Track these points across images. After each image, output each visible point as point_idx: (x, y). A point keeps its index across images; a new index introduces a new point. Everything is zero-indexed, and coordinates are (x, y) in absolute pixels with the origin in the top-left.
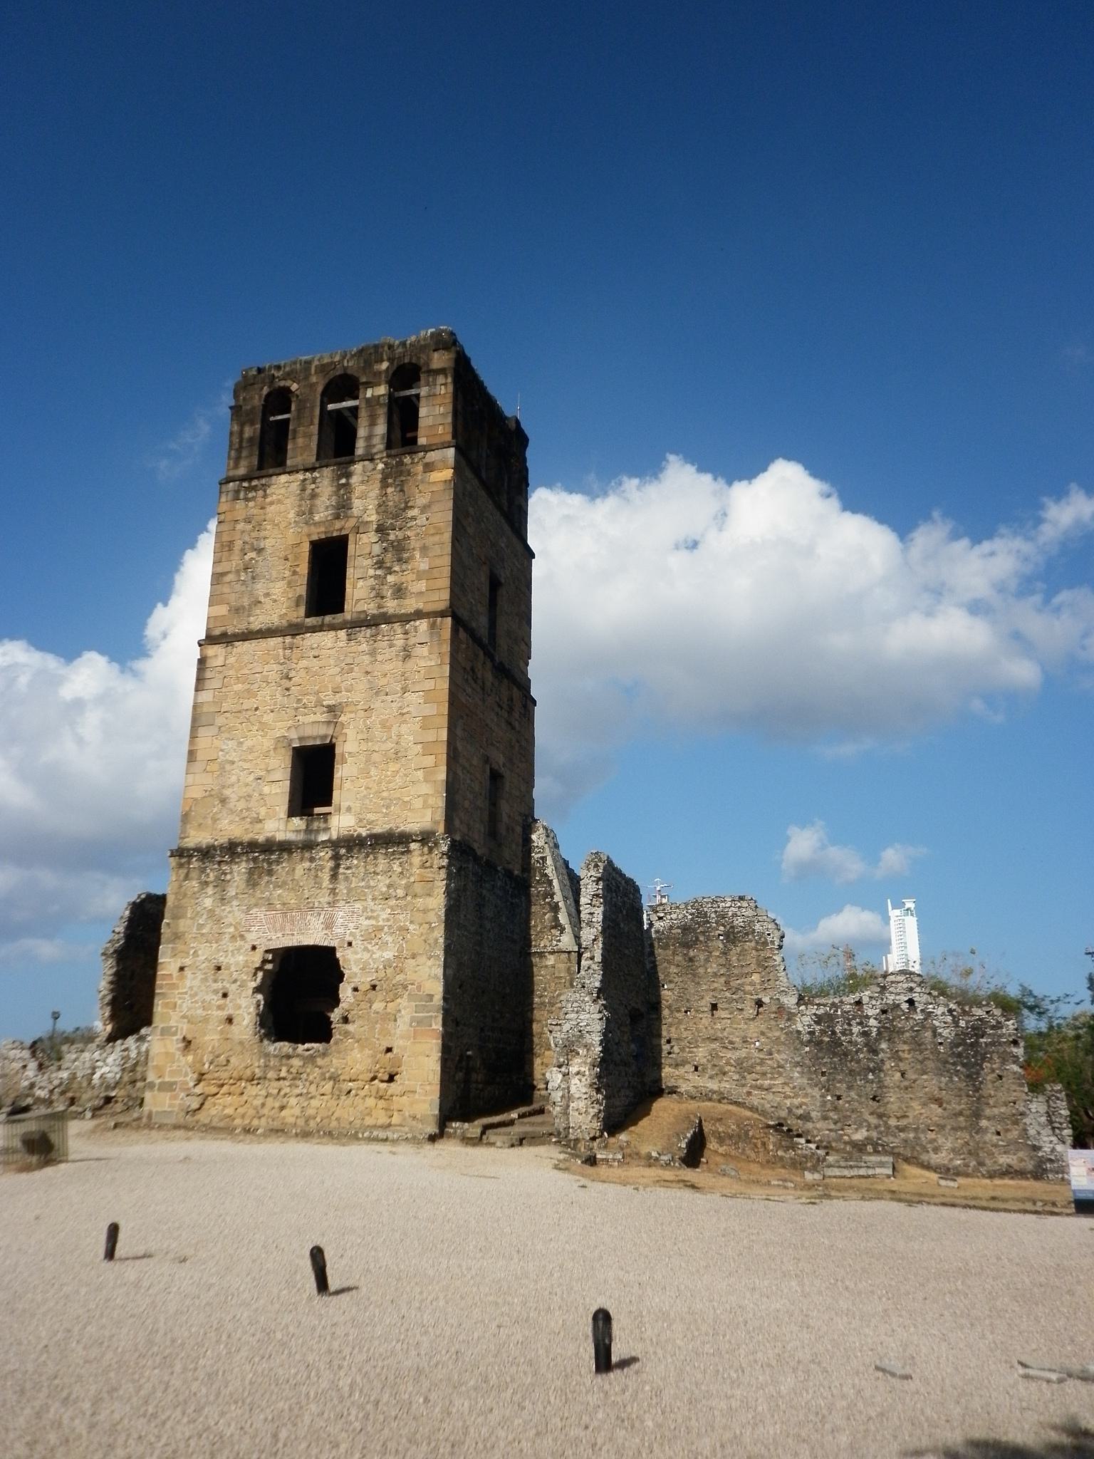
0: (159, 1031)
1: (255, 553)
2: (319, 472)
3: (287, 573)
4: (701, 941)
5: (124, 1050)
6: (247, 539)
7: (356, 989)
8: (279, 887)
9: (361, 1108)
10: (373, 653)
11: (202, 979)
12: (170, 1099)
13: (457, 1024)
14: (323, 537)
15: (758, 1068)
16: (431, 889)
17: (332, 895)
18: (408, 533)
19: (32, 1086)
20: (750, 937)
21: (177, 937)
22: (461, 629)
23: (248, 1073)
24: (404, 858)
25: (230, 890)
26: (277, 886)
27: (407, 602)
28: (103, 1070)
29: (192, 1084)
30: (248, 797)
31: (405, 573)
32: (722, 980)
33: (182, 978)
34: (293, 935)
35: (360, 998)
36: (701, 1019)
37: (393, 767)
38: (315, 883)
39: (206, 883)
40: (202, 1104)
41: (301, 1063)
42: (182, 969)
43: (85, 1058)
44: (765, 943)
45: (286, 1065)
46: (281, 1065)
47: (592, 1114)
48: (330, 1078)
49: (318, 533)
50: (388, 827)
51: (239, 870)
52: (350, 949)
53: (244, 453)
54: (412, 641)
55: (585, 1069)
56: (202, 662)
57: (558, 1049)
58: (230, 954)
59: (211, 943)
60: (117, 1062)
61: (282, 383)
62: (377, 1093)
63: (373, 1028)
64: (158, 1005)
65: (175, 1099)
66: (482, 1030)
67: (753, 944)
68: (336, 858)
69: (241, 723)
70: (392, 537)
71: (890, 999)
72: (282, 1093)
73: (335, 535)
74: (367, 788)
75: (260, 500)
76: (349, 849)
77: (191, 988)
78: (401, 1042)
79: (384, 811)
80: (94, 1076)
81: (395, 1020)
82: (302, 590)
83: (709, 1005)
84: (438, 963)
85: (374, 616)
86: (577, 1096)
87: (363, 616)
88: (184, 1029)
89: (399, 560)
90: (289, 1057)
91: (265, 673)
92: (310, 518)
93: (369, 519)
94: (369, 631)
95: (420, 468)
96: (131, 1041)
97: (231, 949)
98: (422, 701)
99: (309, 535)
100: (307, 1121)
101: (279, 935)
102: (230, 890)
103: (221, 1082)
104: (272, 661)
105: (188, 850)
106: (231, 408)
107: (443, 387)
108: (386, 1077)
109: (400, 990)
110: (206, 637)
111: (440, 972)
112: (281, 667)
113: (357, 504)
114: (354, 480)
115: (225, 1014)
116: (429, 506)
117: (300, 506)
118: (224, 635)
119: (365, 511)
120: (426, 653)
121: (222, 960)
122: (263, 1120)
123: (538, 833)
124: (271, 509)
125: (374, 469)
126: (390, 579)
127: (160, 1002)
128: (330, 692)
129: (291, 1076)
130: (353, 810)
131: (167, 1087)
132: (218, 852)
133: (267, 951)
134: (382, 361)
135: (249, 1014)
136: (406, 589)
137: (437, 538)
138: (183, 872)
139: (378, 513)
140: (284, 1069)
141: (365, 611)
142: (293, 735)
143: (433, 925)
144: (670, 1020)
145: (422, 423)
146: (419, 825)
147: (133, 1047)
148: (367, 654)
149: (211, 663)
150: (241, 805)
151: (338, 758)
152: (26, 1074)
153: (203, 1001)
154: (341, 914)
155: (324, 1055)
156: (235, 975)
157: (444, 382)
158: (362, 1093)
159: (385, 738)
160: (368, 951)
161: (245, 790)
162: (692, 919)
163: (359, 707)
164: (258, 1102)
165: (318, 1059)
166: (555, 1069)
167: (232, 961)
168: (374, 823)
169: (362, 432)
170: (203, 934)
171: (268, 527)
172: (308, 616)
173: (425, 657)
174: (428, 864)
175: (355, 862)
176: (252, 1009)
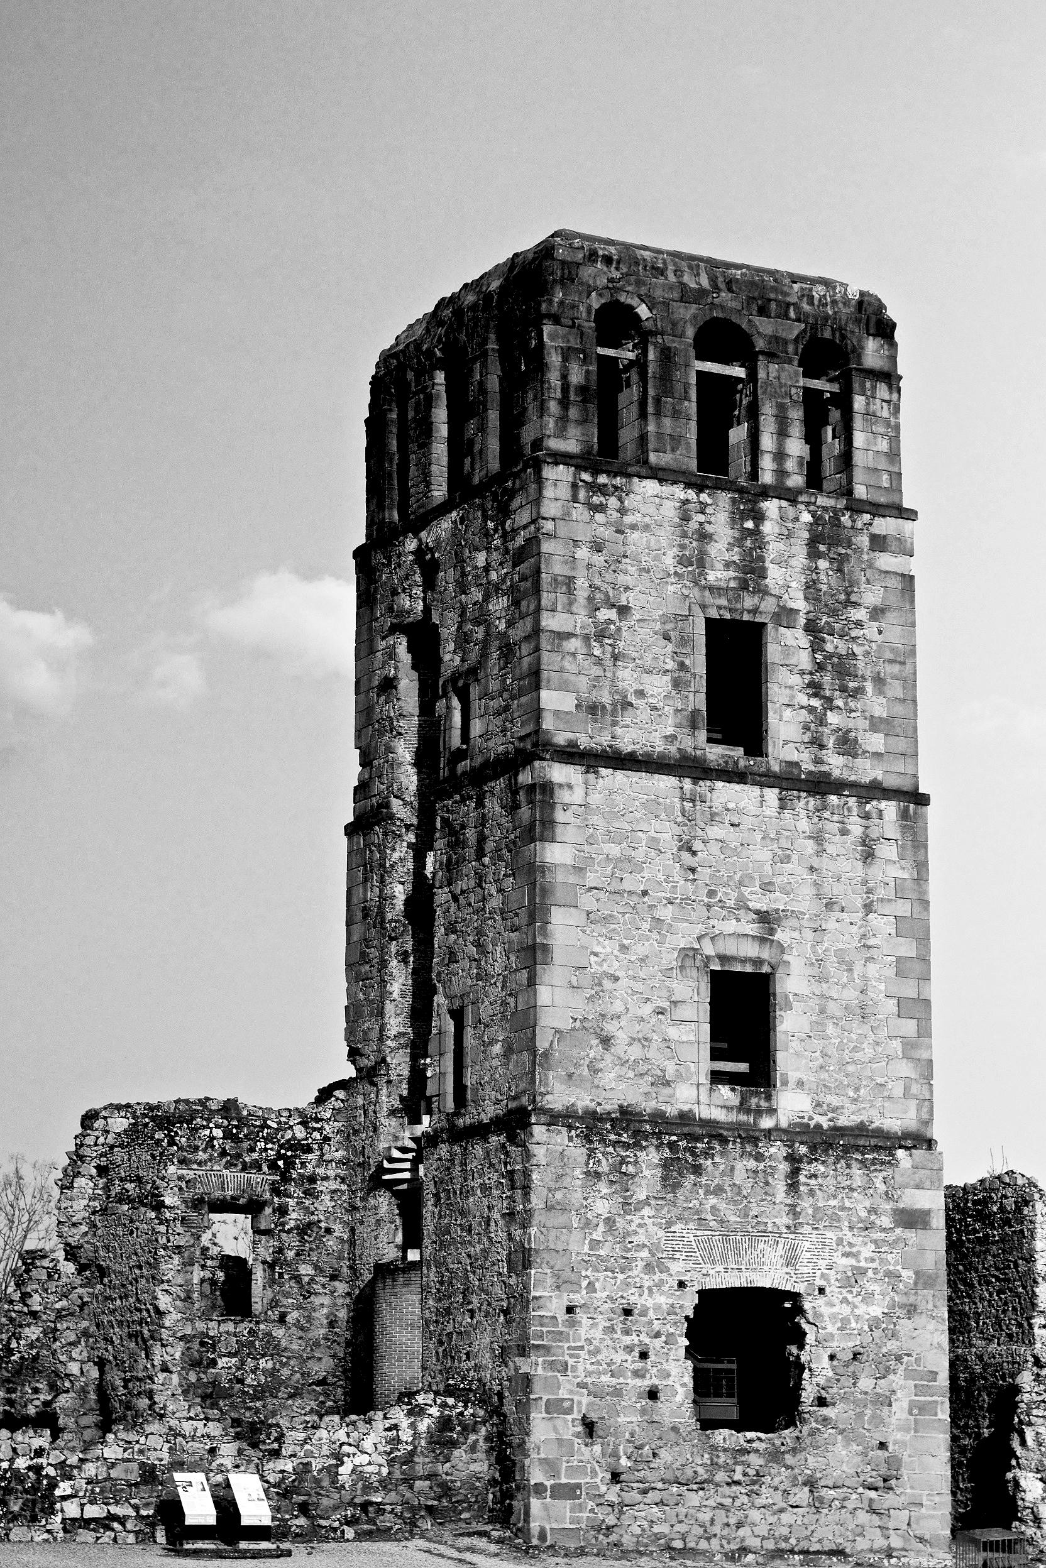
0: (542, 1404)
1: (614, 610)
2: (709, 495)
3: (671, 665)
6: (598, 582)
7: (832, 1357)
8: (712, 1193)
9: (851, 1526)
10: (818, 838)
12: (572, 1510)
14: (727, 616)
17: (791, 1216)
23: (689, 1472)
24: (889, 1172)
25: (637, 1189)
27: (859, 762)
28: (357, 1461)
29: (603, 1489)
31: (853, 715)
33: (573, 1324)
35: (841, 1371)
37: (858, 1028)
39: (598, 1175)
41: (761, 1462)
42: (570, 1310)
43: (320, 1439)
45: (743, 1463)
46: (736, 1463)
49: (719, 608)
51: (650, 1158)
52: (822, 1300)
53: (574, 413)
58: (646, 1292)
59: (613, 1272)
60: (381, 1448)
61: (623, 298)
63: (860, 1416)
68: (792, 1158)
69: (624, 914)
70: (829, 647)
72: (738, 1503)
73: (746, 617)
74: (824, 1055)
76: (813, 1148)
77: (589, 1341)
78: (899, 1436)
79: (851, 1094)
80: (341, 1470)
81: (890, 1405)
82: (699, 701)
84: (940, 1327)
85: (811, 772)
87: (796, 772)
88: (584, 1401)
89: (843, 689)
91: (652, 834)
92: (700, 574)
94: (812, 802)
95: (864, 541)
97: (647, 1284)
98: (893, 932)
99: (703, 607)
101: (720, 1268)
102: (637, 1189)
104: (663, 816)
109: (893, 1363)
111: (944, 1339)
112: (677, 830)
114: (768, 528)
115: (646, 1383)
118: (573, 744)
121: (633, 1298)
122: (715, 1542)
125: (797, 519)
126: (833, 718)
127: (540, 1360)
128: (757, 889)
130: (806, 1087)
131: (568, 1492)
133: (698, 1292)
135: (684, 1385)
136: (856, 741)
137: (895, 669)
139: (806, 599)
141: (796, 764)
142: (709, 949)
145: (859, 458)
146: (899, 1122)
147: (405, 1423)
148: (810, 837)
149: (563, 796)
150: (635, 1052)
154: (807, 1245)
155: (794, 1451)
156: (657, 1326)
157: (887, 397)
159: (845, 980)
161: (638, 1028)
163: (805, 923)
164: (705, 1517)
165: (787, 1456)
166: (1031, 1475)
167: (650, 1303)
168: (839, 1111)
169: (767, 442)
171: (632, 570)
175: (822, 1168)
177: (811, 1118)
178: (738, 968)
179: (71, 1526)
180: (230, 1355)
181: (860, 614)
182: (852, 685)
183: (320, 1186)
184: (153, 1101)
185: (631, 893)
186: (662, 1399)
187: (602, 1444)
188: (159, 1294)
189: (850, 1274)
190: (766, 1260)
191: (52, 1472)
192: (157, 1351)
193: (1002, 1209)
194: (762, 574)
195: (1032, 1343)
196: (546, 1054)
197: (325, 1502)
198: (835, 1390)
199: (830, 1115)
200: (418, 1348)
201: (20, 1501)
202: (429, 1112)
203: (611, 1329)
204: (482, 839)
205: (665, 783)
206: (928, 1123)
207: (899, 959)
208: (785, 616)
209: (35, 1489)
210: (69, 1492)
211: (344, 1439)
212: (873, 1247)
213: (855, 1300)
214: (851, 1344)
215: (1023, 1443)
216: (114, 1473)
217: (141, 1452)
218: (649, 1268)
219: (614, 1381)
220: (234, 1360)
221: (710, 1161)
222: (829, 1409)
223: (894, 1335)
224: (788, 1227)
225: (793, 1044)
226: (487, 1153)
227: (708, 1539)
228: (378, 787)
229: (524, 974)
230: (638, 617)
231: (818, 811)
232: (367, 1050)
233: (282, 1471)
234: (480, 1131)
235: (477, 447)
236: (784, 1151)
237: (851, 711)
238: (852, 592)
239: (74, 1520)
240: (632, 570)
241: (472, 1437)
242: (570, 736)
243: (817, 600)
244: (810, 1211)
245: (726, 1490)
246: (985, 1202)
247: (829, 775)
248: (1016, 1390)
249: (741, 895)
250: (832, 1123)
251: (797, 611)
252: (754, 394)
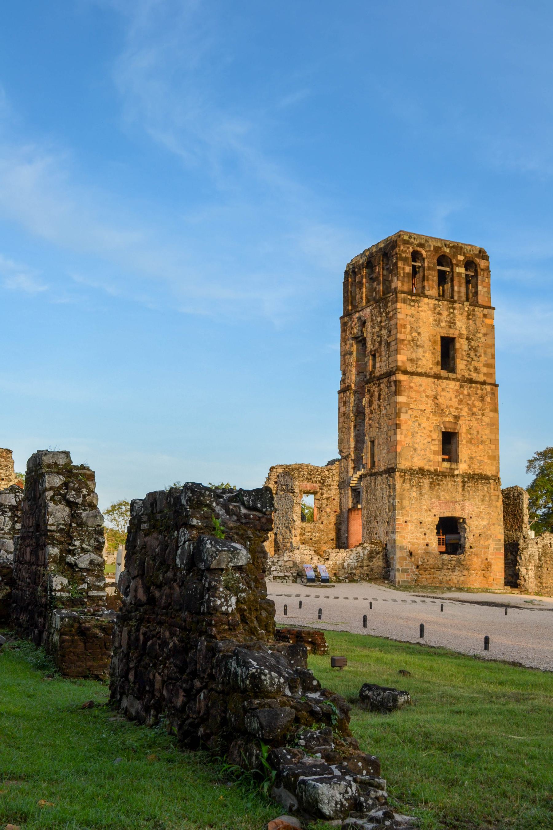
3: (431, 348)
7: (474, 535)
21: (403, 508)
23: (437, 566)
24: (488, 485)
29: (415, 570)
33: (407, 526)
39: (413, 486)
51: (426, 482)
52: (471, 520)
55: (533, 568)
63: (481, 551)
68: (463, 482)
70: (473, 343)
71: (545, 542)
73: (451, 336)
76: (469, 479)
78: (490, 557)
85: (467, 378)
89: (476, 355)
90: (451, 560)
93: (463, 333)
113: (458, 324)
115: (426, 542)
124: (422, 313)
138: (402, 479)
140: (449, 565)
147: (361, 552)
149: (404, 384)
150: (423, 453)
153: (416, 536)
164: (440, 578)
167: (427, 520)
169: (456, 288)
179: (275, 578)
180: (309, 532)
181: (480, 335)
182: (478, 354)
183: (332, 487)
184: (288, 464)
188: (294, 516)
192: (293, 531)
193: (513, 496)
194: (455, 324)
195: (522, 532)
196: (399, 453)
200: (361, 531)
202: (363, 467)
204: (380, 395)
205: (431, 380)
206: (498, 473)
208: (460, 335)
210: (275, 569)
215: (521, 559)
216: (286, 564)
219: (417, 541)
220: (310, 534)
223: (490, 530)
226: (382, 479)
228: (347, 381)
229: (393, 432)
232: (344, 451)
234: (381, 474)
235: (377, 289)
239: (276, 577)
240: (421, 322)
241: (378, 556)
243: (469, 331)
245: (446, 570)
246: (508, 494)
248: (519, 545)
252: (453, 275)
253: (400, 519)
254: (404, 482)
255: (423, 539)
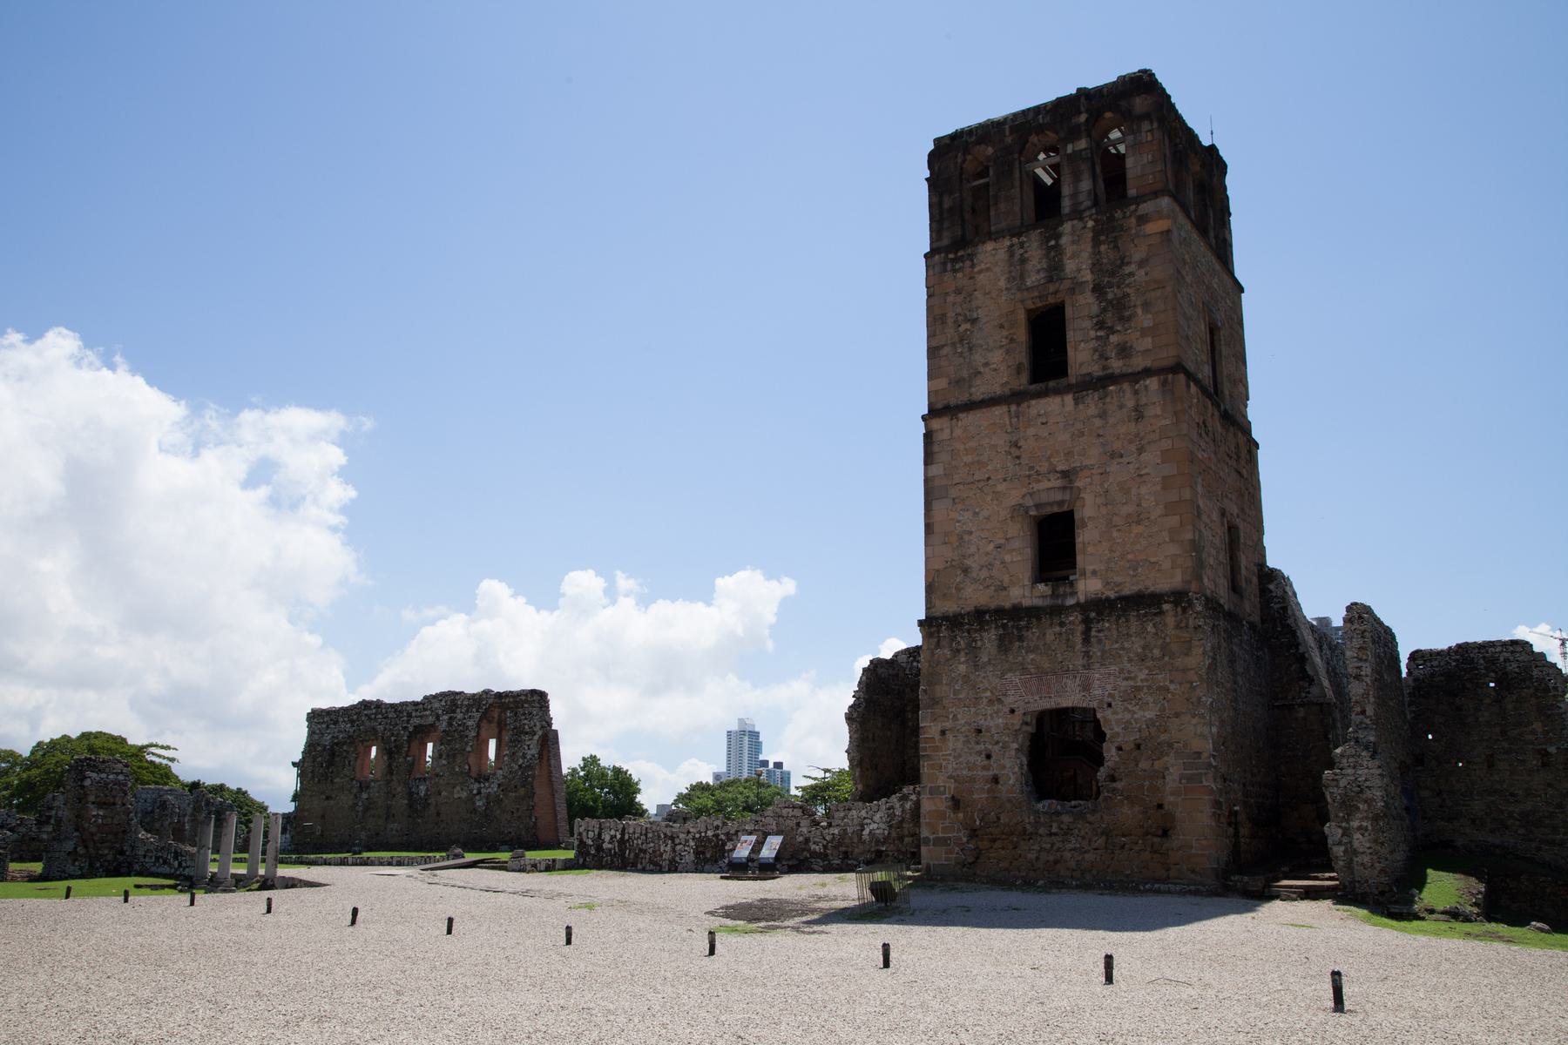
3: (1005, 342)
4: (1468, 689)
5: (889, 809)
6: (959, 310)
7: (1119, 749)
10: (1103, 415)
11: (964, 741)
12: (946, 853)
13: (1225, 780)
15: (1547, 822)
16: (1190, 649)
18: (1128, 290)
19: (807, 840)
20: (1528, 683)
21: (935, 702)
22: (1192, 384)
24: (1158, 619)
26: (1029, 651)
28: (871, 827)
29: (965, 839)
30: (990, 566)
32: (1498, 729)
34: (1050, 697)
36: (1475, 770)
37: (1137, 529)
38: (1067, 647)
39: (958, 651)
40: (977, 858)
42: (943, 733)
44: (1547, 690)
46: (1052, 821)
47: (1378, 869)
48: (1102, 834)
50: (1135, 589)
52: (1109, 711)
53: (946, 225)
54: (1143, 401)
56: (928, 437)
57: (1336, 804)
62: (1152, 846)
64: (923, 766)
65: (951, 853)
66: (1244, 785)
67: (1532, 690)
68: (1087, 622)
70: (1110, 296)
72: (1055, 848)
73: (1051, 300)
74: (1111, 551)
75: (967, 270)
76: (1099, 614)
77: (954, 750)
79: (1131, 573)
80: (864, 833)
81: (1164, 778)
82: (1022, 355)
83: (1484, 756)
84: (1203, 721)
85: (1100, 379)
86: (1361, 850)
87: (1087, 379)
89: (1121, 319)
90: (1058, 813)
93: (1084, 279)
94: (1096, 395)
95: (1133, 220)
96: (894, 799)
97: (989, 712)
98: (1159, 461)
99: (1022, 301)
100: (1083, 874)
103: (994, 837)
105: (936, 618)
106: (926, 179)
107: (1149, 134)
108: (1160, 832)
110: (929, 411)
113: (1070, 266)
114: (1064, 240)
115: (991, 773)
116: (1147, 260)
117: (1010, 272)
119: (1079, 270)
120: (1159, 413)
123: (1275, 582)
125: (1085, 227)
126: (1114, 339)
127: (926, 764)
129: (1063, 833)
132: (966, 621)
133: (1024, 714)
134: (1080, 113)
135: (1013, 773)
136: (1131, 347)
137: (1158, 293)
139: (1092, 272)
140: (1055, 825)
142: (1029, 502)
143: (1194, 684)
144: (1439, 772)
145: (1130, 174)
147: (898, 805)
149: (938, 437)
150: (984, 574)
151: (1077, 523)
152: (800, 829)
154: (1097, 676)
155: (1093, 812)
156: (996, 737)
157: (1149, 128)
158: (1137, 848)
160: (1129, 711)
161: (985, 559)
162: (1455, 666)
164: (1032, 856)
165: (1088, 816)
167: (992, 724)
170: (959, 699)
172: (1031, 384)
173: (1159, 416)
174: (1183, 625)
175: (1107, 625)
176: (1016, 769)
177: (1103, 593)
178: (1048, 510)
185: (979, 481)
186: (1001, 782)
187: (964, 813)
189: (1129, 691)
190: (1068, 689)
191: (723, 837)
197: (856, 850)
198: (1122, 770)
199: (1116, 589)
201: (710, 853)
203: (968, 742)
205: (999, 411)
207: (1164, 478)
209: (716, 845)
211: (865, 815)
212: (1147, 671)
213: (1134, 708)
214: (1132, 739)
217: (763, 826)
218: (991, 702)
219: (970, 774)
221: (1029, 633)
222: (1117, 783)
224: (1084, 666)
225: (1089, 549)
227: (1034, 870)
230: (984, 320)
231: (1101, 399)
233: (833, 834)
236: (1080, 617)
237: (1126, 330)
238: (1125, 257)
242: (945, 402)
244: (1099, 654)
247: (1113, 373)
249: (1051, 464)
250: (1116, 595)
251: (1088, 282)
253: (930, 728)
254: (938, 645)
255: (985, 768)
